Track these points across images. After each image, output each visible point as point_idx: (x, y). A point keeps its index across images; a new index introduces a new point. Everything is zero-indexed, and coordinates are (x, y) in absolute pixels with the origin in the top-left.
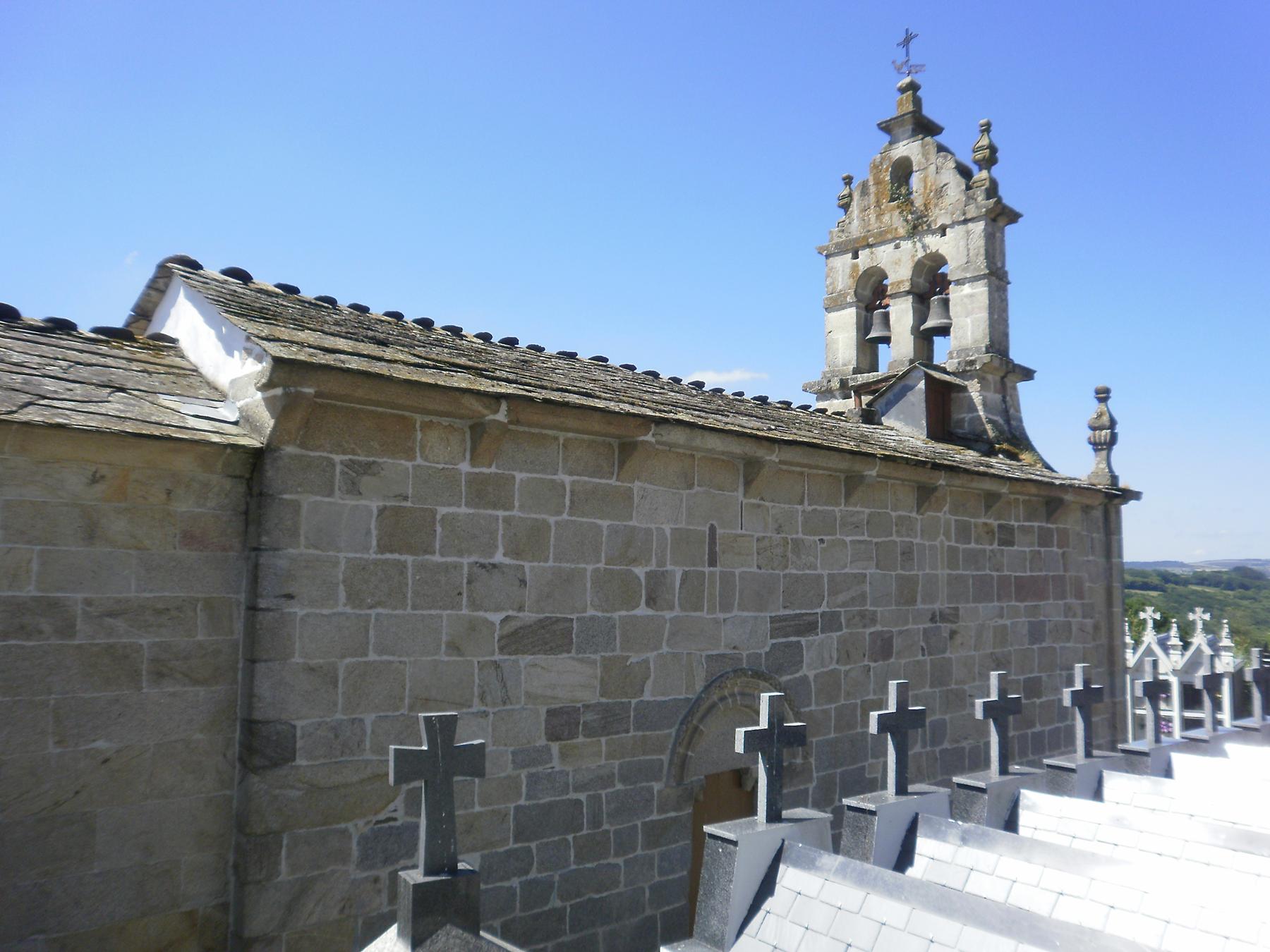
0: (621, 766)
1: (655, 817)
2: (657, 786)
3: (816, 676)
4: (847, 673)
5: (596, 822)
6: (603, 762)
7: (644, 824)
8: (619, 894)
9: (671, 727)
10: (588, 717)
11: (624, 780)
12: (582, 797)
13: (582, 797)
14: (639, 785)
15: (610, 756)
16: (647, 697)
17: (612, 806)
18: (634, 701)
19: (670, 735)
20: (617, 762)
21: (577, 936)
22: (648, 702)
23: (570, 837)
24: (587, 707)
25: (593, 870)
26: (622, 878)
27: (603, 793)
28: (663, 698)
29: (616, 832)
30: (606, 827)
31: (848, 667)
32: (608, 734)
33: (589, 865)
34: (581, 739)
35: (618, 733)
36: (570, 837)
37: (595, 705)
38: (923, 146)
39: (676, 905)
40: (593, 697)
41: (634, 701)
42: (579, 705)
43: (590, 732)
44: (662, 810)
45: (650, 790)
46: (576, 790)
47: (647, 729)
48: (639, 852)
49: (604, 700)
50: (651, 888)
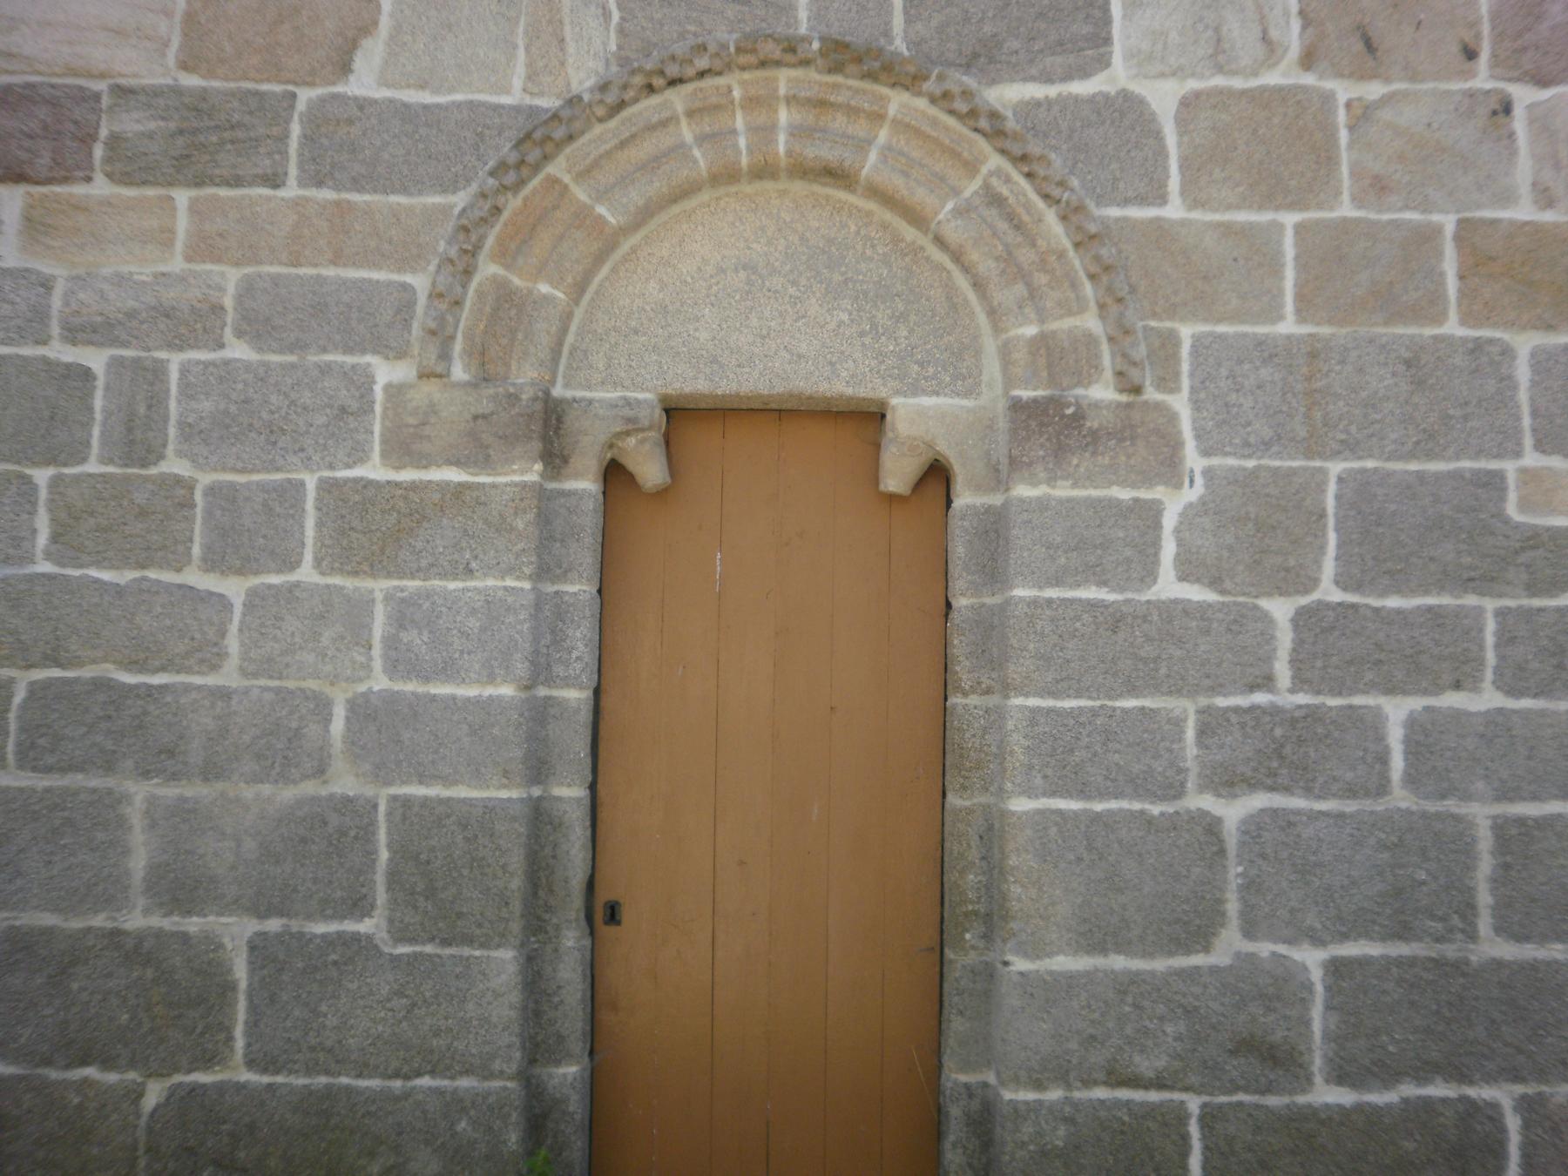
0: (248, 289)
1: (375, 470)
2: (385, 373)
3: (1189, 103)
4: (1362, 114)
5: (137, 443)
6: (177, 264)
7: (328, 487)
8: (224, 694)
9: (452, 187)
10: (132, 123)
11: (255, 328)
12: (96, 360)
13: (96, 360)
14: (313, 358)
15: (203, 248)
16: (363, 83)
17: (206, 405)
18: (305, 95)
19: (445, 210)
20: (232, 277)
21: (42, 782)
22: (363, 104)
23: (42, 476)
24: (122, 92)
25: (119, 591)
26: (233, 644)
27: (175, 361)
28: (427, 98)
29: (211, 491)
30: (174, 465)
31: (1374, 90)
32: (199, 183)
33: (106, 576)
34: (100, 187)
35: (237, 182)
36: (42, 476)
37: (157, 92)
38: (514, 819)
39: (462, 792)
40: (158, 69)
41: (305, 95)
42: (101, 86)
43: (131, 166)
44: (402, 448)
45: (365, 382)
46: (73, 334)
47: (357, 185)
48: (306, 573)
49: (191, 81)
50: (353, 706)
